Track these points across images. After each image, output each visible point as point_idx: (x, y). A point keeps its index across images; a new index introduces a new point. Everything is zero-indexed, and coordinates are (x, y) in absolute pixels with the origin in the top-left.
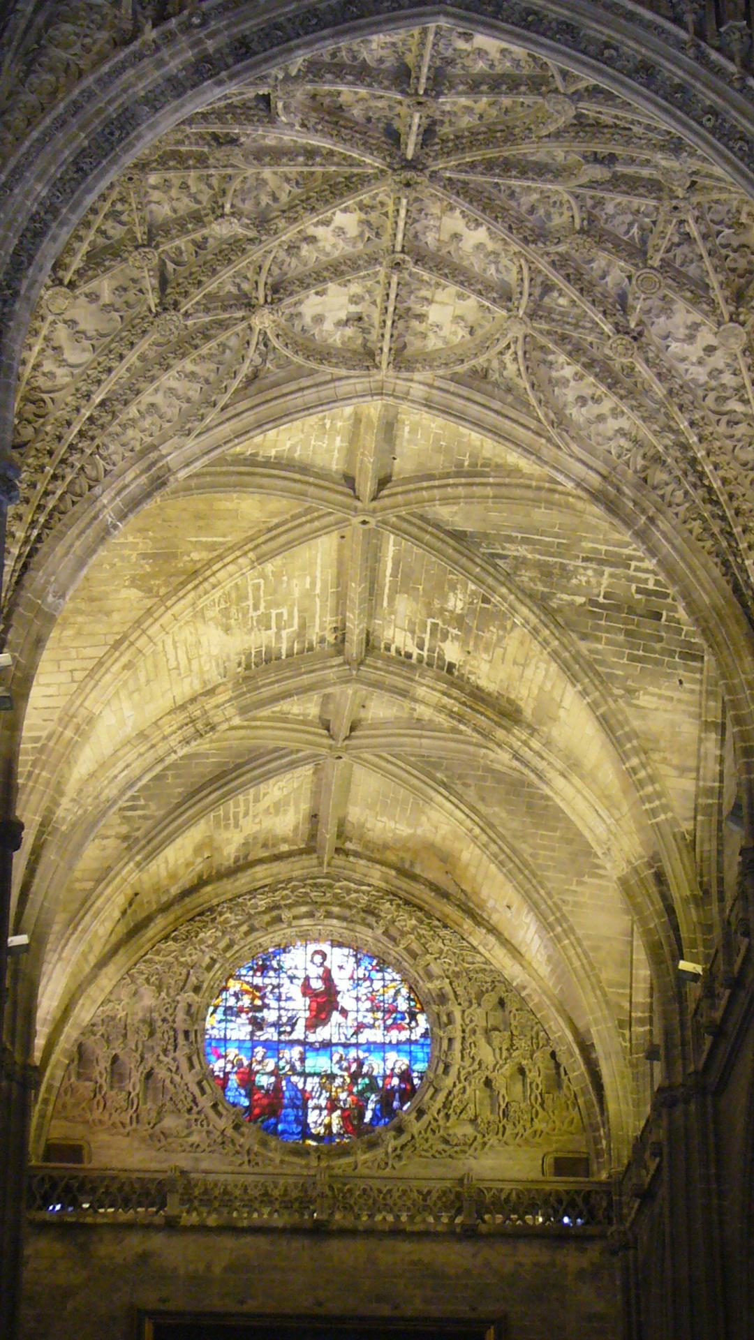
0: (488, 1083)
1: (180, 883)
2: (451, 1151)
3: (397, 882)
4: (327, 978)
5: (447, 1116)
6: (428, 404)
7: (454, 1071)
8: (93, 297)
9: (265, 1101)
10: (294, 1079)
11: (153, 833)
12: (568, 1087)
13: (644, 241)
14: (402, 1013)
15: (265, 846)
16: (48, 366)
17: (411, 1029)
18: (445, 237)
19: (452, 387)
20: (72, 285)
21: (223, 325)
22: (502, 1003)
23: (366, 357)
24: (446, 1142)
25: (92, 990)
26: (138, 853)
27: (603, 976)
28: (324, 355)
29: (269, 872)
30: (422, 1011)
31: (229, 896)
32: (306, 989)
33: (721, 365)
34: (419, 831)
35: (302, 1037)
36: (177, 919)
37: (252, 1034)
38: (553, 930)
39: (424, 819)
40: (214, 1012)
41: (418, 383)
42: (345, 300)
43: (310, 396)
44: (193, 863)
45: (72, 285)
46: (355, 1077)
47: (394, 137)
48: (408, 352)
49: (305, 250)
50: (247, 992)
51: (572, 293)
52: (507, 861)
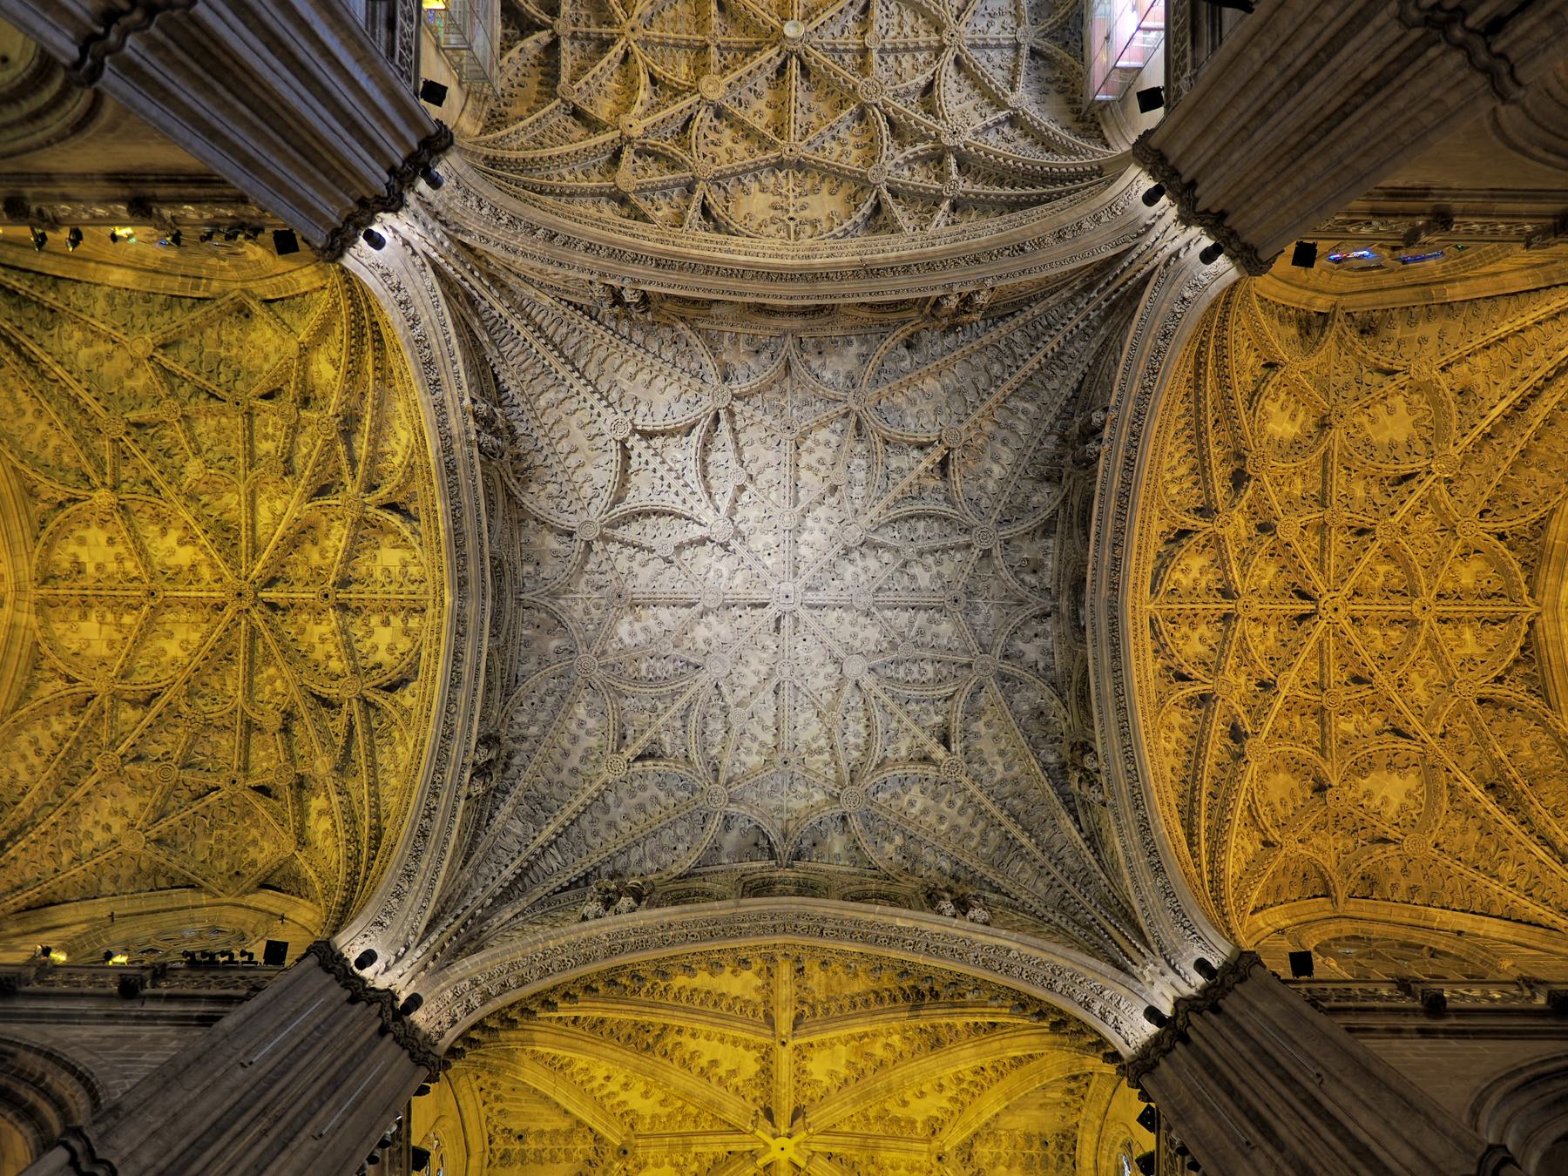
6: (13, 626)
8: (130, 374)
13: (190, 766)
16: (78, 335)
18: (168, 627)
19: (28, 644)
20: (151, 358)
21: (100, 468)
23: (46, 579)
28: (49, 546)
33: (96, 838)
41: (27, 618)
42: (100, 559)
43: (18, 536)
45: (151, 358)
47: (271, 583)
48: (50, 611)
49: (156, 528)
51: (150, 717)
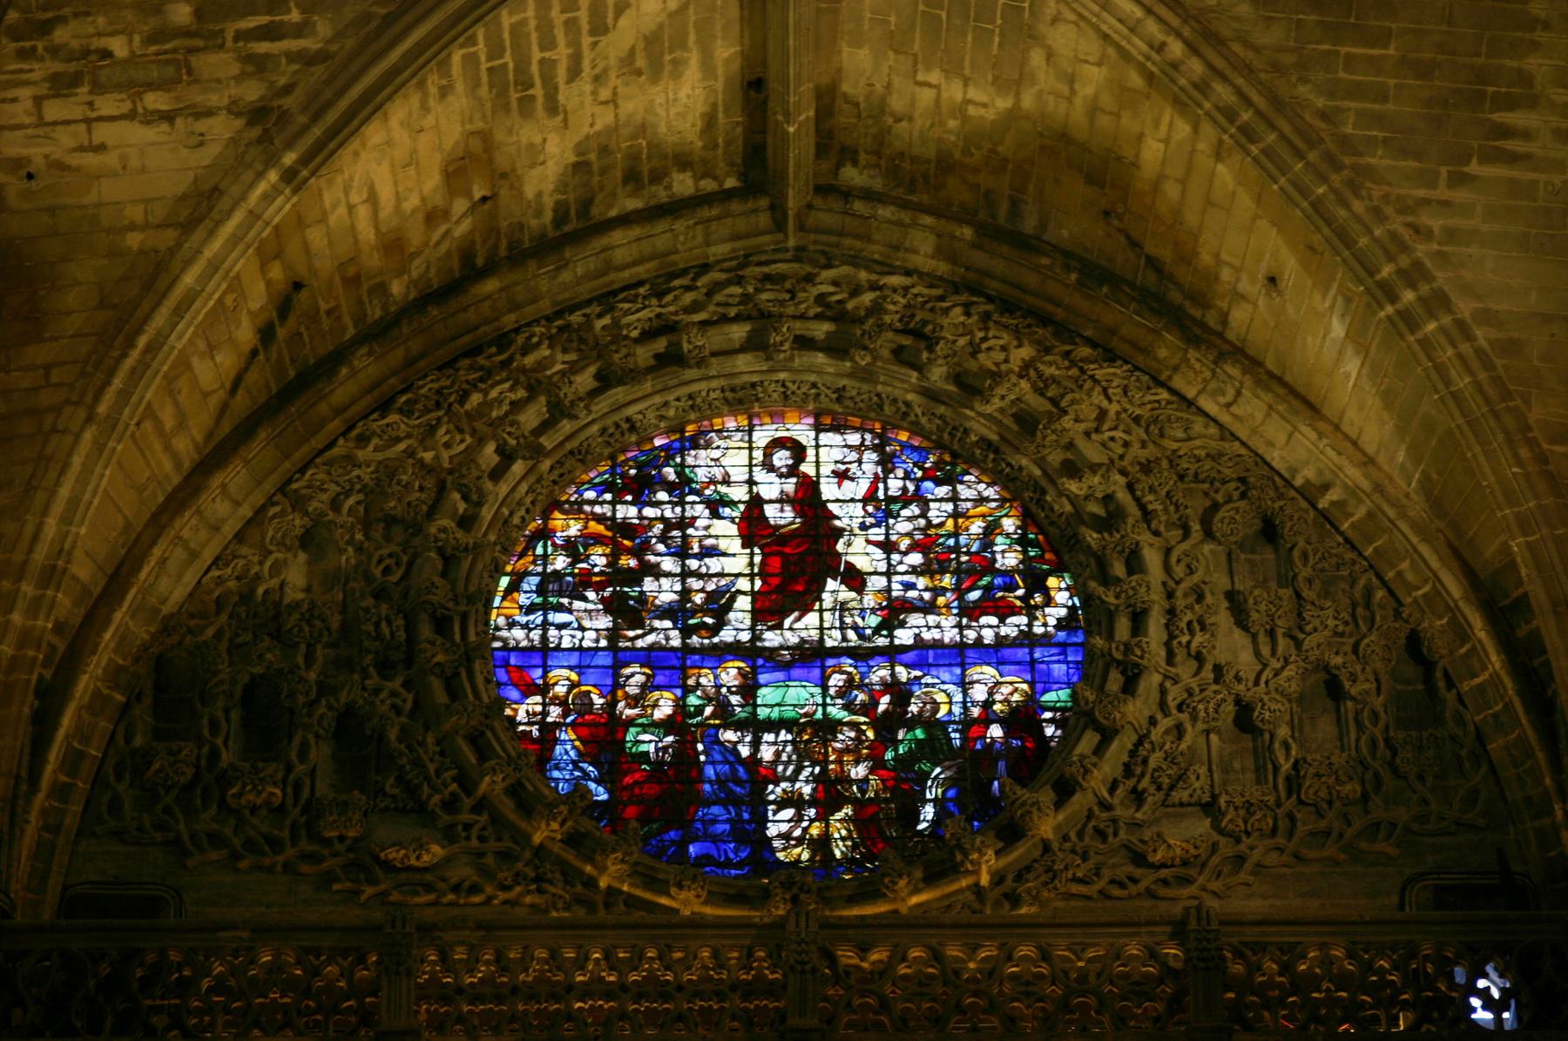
0: (1245, 718)
1: (416, 268)
2: (1148, 879)
3: (980, 259)
4: (807, 497)
5: (1138, 797)
7: (1150, 682)
9: (652, 790)
10: (729, 735)
11: (328, 94)
12: (1460, 720)
14: (1007, 573)
15: (632, 177)
17: (1031, 611)
22: (1269, 531)
24: (1139, 859)
25: (187, 525)
26: (289, 145)
27: (1535, 415)
29: (646, 247)
30: (1058, 571)
31: (546, 306)
32: (753, 525)
34: (1028, 101)
35: (745, 637)
36: (409, 363)
37: (613, 634)
38: (1393, 298)
39: (1037, 57)
40: (514, 587)
44: (446, 214)
46: (887, 726)
50: (598, 539)
52: (1260, 127)
